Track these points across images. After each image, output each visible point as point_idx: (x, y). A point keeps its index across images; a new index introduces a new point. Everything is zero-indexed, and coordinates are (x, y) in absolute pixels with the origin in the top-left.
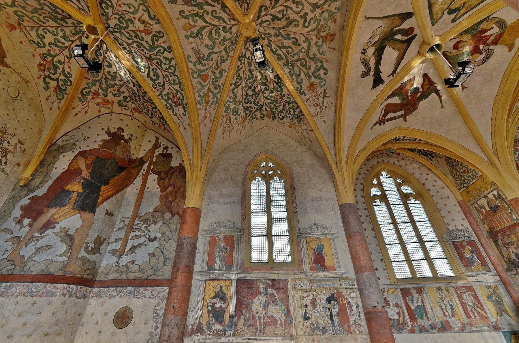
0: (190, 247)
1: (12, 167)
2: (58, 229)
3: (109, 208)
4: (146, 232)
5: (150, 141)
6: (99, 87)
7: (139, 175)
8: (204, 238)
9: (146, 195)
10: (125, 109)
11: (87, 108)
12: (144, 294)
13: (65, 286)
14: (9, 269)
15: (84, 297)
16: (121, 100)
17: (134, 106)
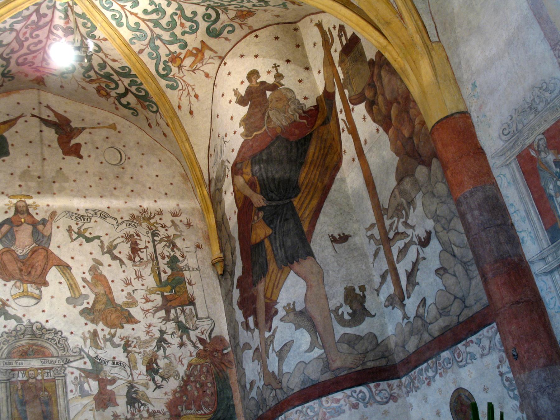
0: (481, 215)
2: (282, 313)
3: (331, 228)
4: (410, 232)
5: (315, 45)
6: (164, 44)
7: (341, 129)
8: (506, 171)
9: (372, 159)
10: (229, 32)
11: (190, 89)
12: (470, 353)
13: (348, 392)
14: (274, 397)
15: (393, 398)
16: (208, 29)
17: (232, 14)
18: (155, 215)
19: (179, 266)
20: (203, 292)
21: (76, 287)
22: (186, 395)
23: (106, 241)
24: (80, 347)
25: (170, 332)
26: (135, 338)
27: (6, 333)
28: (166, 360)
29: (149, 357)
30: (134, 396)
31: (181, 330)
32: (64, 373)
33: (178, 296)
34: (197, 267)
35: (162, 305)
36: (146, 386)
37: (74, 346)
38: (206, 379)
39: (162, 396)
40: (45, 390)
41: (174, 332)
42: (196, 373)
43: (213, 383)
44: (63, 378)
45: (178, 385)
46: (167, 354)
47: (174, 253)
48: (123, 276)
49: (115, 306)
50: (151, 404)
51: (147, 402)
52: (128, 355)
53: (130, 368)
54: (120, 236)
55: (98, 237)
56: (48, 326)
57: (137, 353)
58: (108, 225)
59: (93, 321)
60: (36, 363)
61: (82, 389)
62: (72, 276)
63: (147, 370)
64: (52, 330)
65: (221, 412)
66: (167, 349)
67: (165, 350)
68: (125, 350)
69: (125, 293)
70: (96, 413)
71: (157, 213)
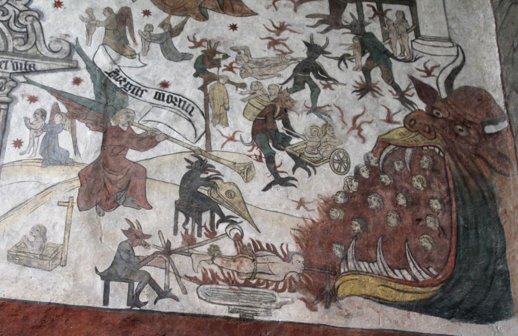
22: (360, 217)
24: (72, 40)
26: (233, 49)
28: (314, 117)
29: (267, 101)
30: (204, 190)
31: (368, 55)
37: (58, 36)
38: (428, 188)
39: (287, 208)
41: (349, 55)
42: (398, 167)
43: (446, 203)
45: (340, 187)
46: (319, 104)
50: (251, 222)
51: (240, 215)
52: (205, 84)
53: (206, 117)
57: (233, 83)
63: (254, 133)
66: (323, 91)
67: (315, 92)
70: (76, 213)
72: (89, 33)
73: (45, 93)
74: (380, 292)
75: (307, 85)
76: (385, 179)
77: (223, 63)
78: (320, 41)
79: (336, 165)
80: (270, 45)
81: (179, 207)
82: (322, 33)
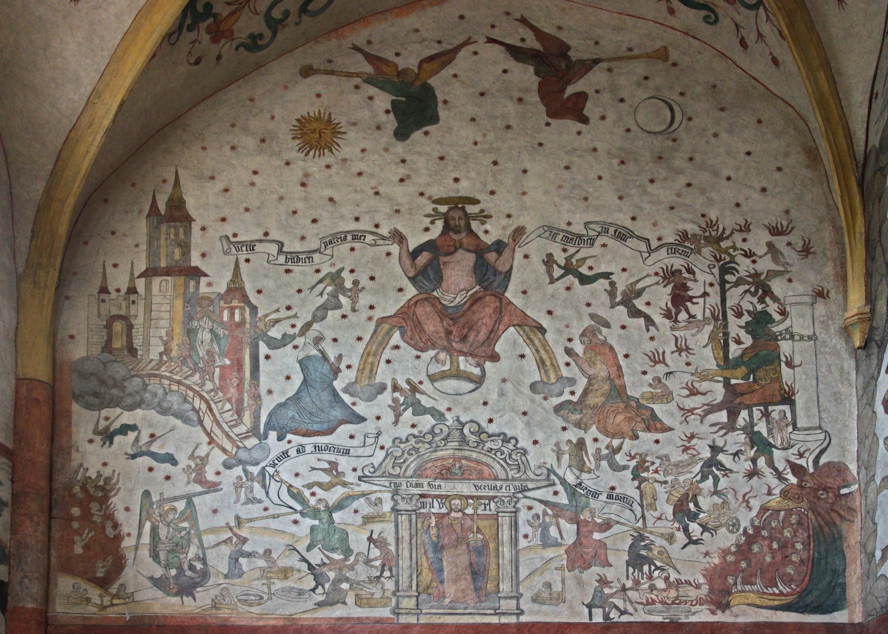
1: (808, 310)
18: (732, 233)
19: (770, 330)
20: (814, 382)
21: (553, 365)
23: (622, 282)
24: (549, 466)
25: (733, 450)
27: (415, 437)
28: (715, 498)
29: (682, 491)
30: (643, 552)
31: (755, 448)
32: (514, 507)
33: (759, 387)
34: (811, 333)
35: (722, 402)
36: (671, 538)
37: (539, 464)
39: (698, 558)
40: (479, 531)
41: (741, 450)
44: (513, 515)
45: (733, 542)
47: (764, 305)
48: (649, 347)
49: (625, 399)
51: (667, 565)
53: (642, 506)
54: (652, 272)
55: (606, 275)
56: (492, 428)
58: (628, 252)
59: (578, 425)
60: (466, 488)
61: (545, 535)
62: (545, 344)
64: (499, 435)
65: (815, 593)
66: (722, 479)
67: (716, 480)
68: (636, 476)
69: (648, 378)
71: (738, 228)
72: (559, 459)
73: (536, 504)
74: (758, 602)
75: (710, 476)
76: (764, 533)
77: (651, 468)
78: (720, 443)
79: (731, 528)
80: (684, 451)
81: (628, 564)
82: (721, 436)
